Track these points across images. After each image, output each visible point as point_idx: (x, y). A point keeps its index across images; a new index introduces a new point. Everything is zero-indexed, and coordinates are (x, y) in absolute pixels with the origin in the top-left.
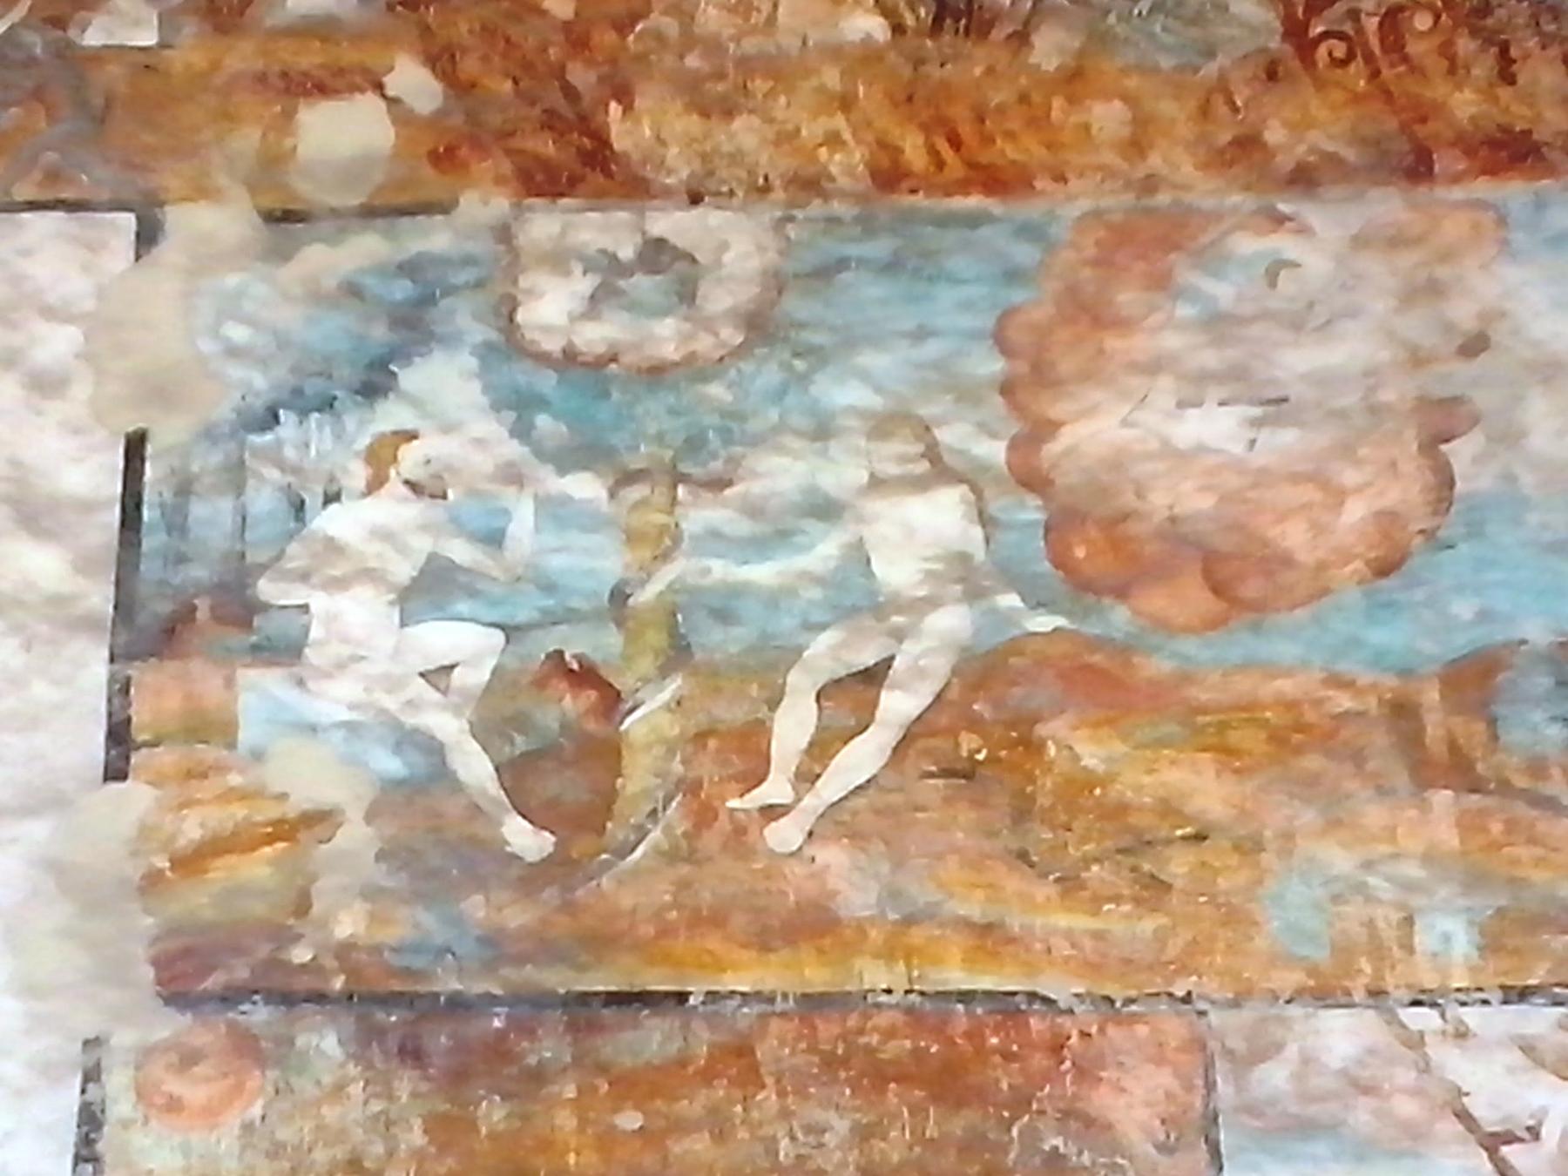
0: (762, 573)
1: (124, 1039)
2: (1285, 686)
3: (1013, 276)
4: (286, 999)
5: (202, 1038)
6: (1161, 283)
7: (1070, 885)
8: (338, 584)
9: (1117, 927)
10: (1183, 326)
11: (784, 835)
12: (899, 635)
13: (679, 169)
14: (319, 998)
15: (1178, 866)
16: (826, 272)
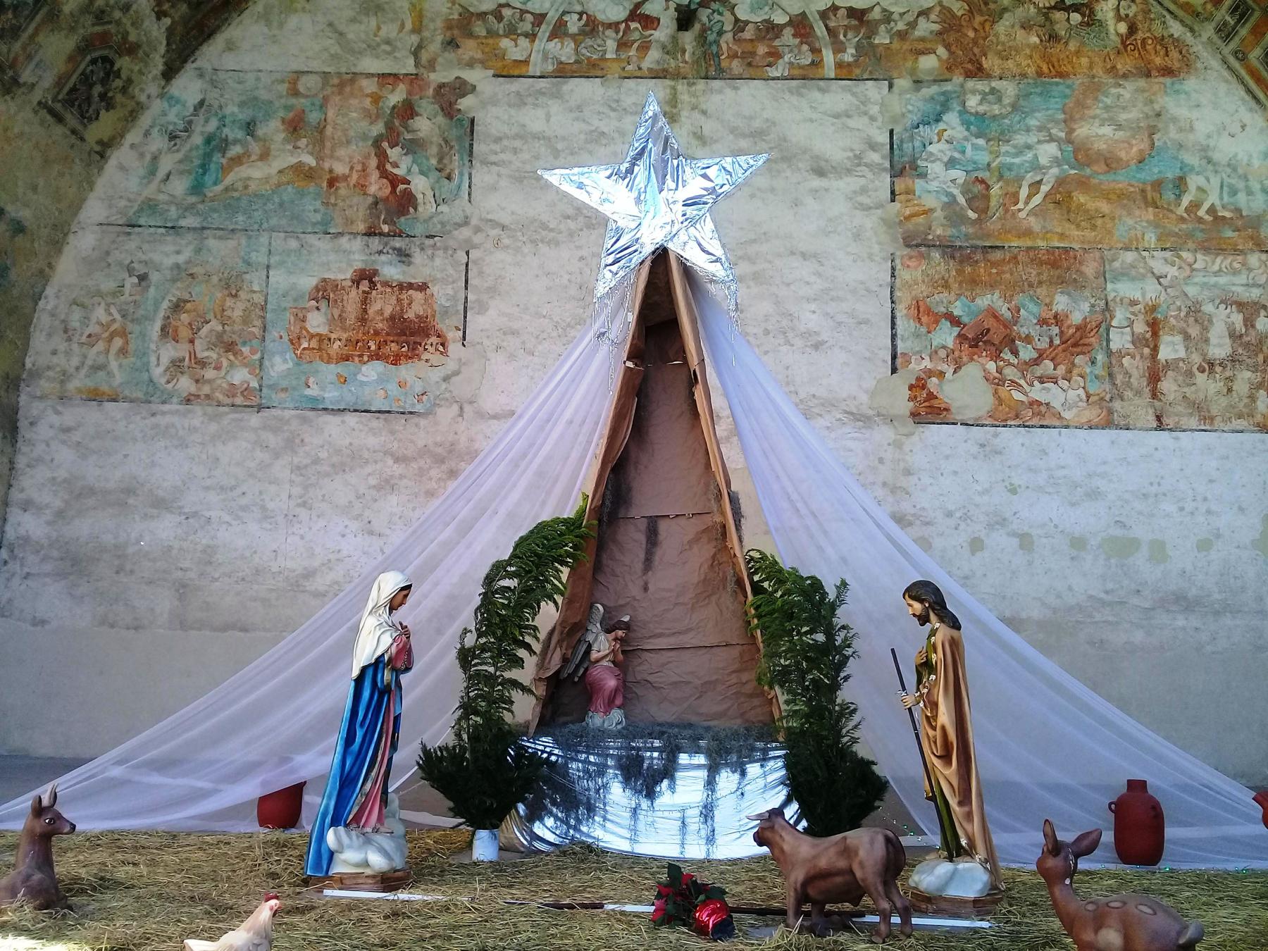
0: (1017, 160)
1: (898, 253)
2: (1120, 186)
3: (1066, 97)
4: (929, 246)
5: (914, 252)
6: (1096, 99)
7: (1078, 226)
8: (933, 162)
9: (1087, 234)
10: (1101, 109)
11: (1022, 215)
12: (1044, 174)
13: (997, 72)
14: (934, 246)
15: (1099, 222)
16: (1028, 95)
